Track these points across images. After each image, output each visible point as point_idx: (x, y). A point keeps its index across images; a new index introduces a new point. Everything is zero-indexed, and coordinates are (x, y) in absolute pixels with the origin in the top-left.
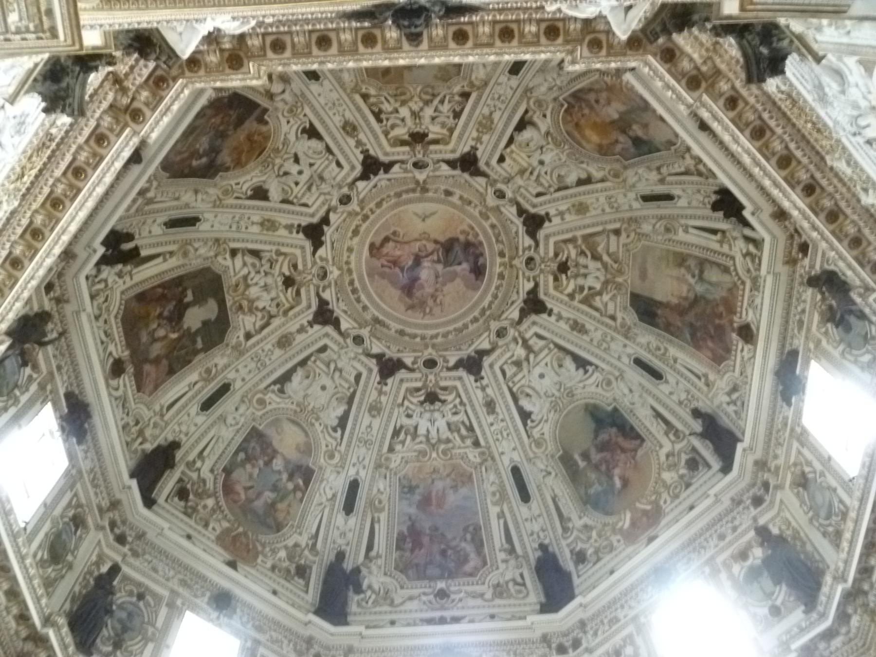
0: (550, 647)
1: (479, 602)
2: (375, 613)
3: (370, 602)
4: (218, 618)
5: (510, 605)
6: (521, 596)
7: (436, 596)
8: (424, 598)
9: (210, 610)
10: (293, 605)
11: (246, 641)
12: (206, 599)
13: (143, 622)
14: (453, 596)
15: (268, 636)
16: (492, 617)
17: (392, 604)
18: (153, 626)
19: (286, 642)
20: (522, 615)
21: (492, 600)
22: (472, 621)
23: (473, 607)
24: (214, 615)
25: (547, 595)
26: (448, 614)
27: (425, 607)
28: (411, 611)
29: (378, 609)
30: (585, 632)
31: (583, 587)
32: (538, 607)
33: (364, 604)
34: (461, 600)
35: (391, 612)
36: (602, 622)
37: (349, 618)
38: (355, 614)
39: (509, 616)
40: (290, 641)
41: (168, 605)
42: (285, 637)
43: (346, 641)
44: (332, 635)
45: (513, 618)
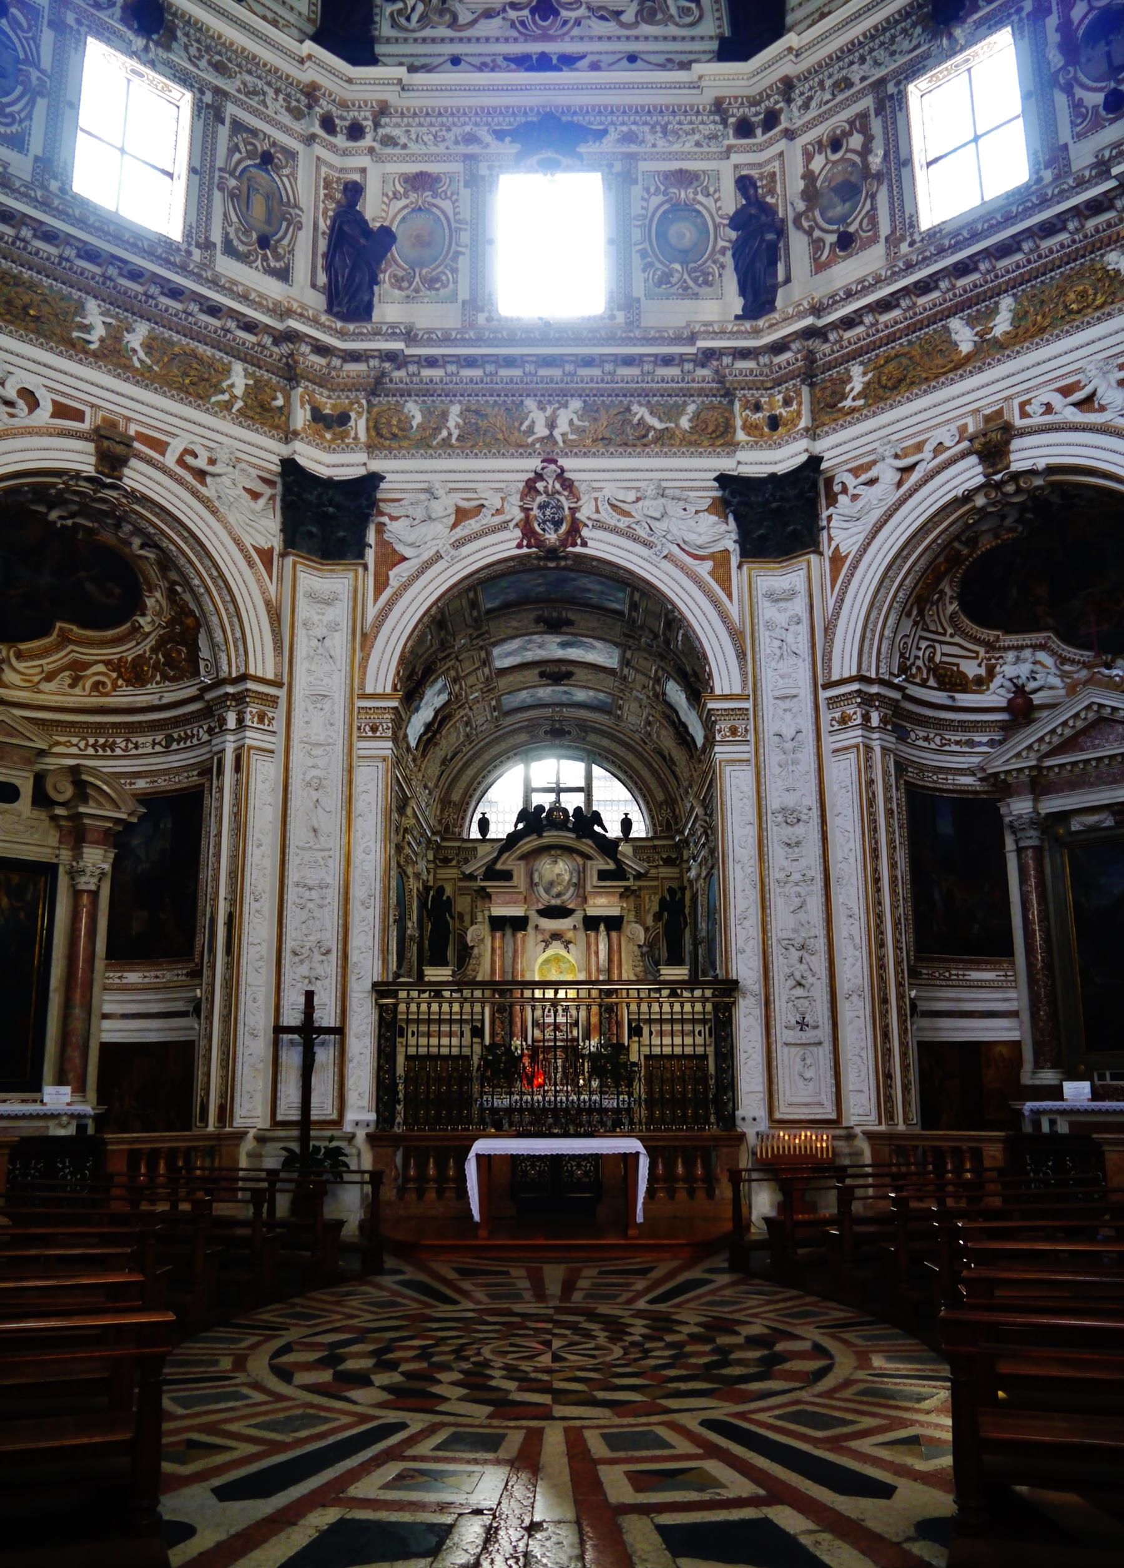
0: (724, 122)
1: (609, 28)
2: (424, 40)
3: (415, 17)
4: (146, 49)
5: (665, 38)
6: (688, 20)
7: (533, 12)
8: (512, 14)
9: (130, 35)
10: (274, 23)
11: (202, 92)
12: (117, 11)
13: (17, 61)
14: (564, 14)
15: (238, 83)
16: (632, 58)
17: (453, 23)
18: (38, 67)
19: (271, 92)
20: (685, 58)
21: (636, 24)
22: (595, 67)
23: (600, 38)
24: (139, 42)
25: (734, 23)
26: (552, 48)
27: (515, 34)
28: (487, 40)
29: (427, 32)
30: (789, 101)
31: (799, 14)
32: (714, 45)
33: (402, 21)
34: (578, 22)
35: (452, 40)
36: (821, 84)
37: (379, 49)
38: (388, 41)
39: (660, 59)
40: (278, 91)
41: (51, 24)
42: (269, 84)
43: (375, 95)
44: (350, 81)
45: (669, 64)
